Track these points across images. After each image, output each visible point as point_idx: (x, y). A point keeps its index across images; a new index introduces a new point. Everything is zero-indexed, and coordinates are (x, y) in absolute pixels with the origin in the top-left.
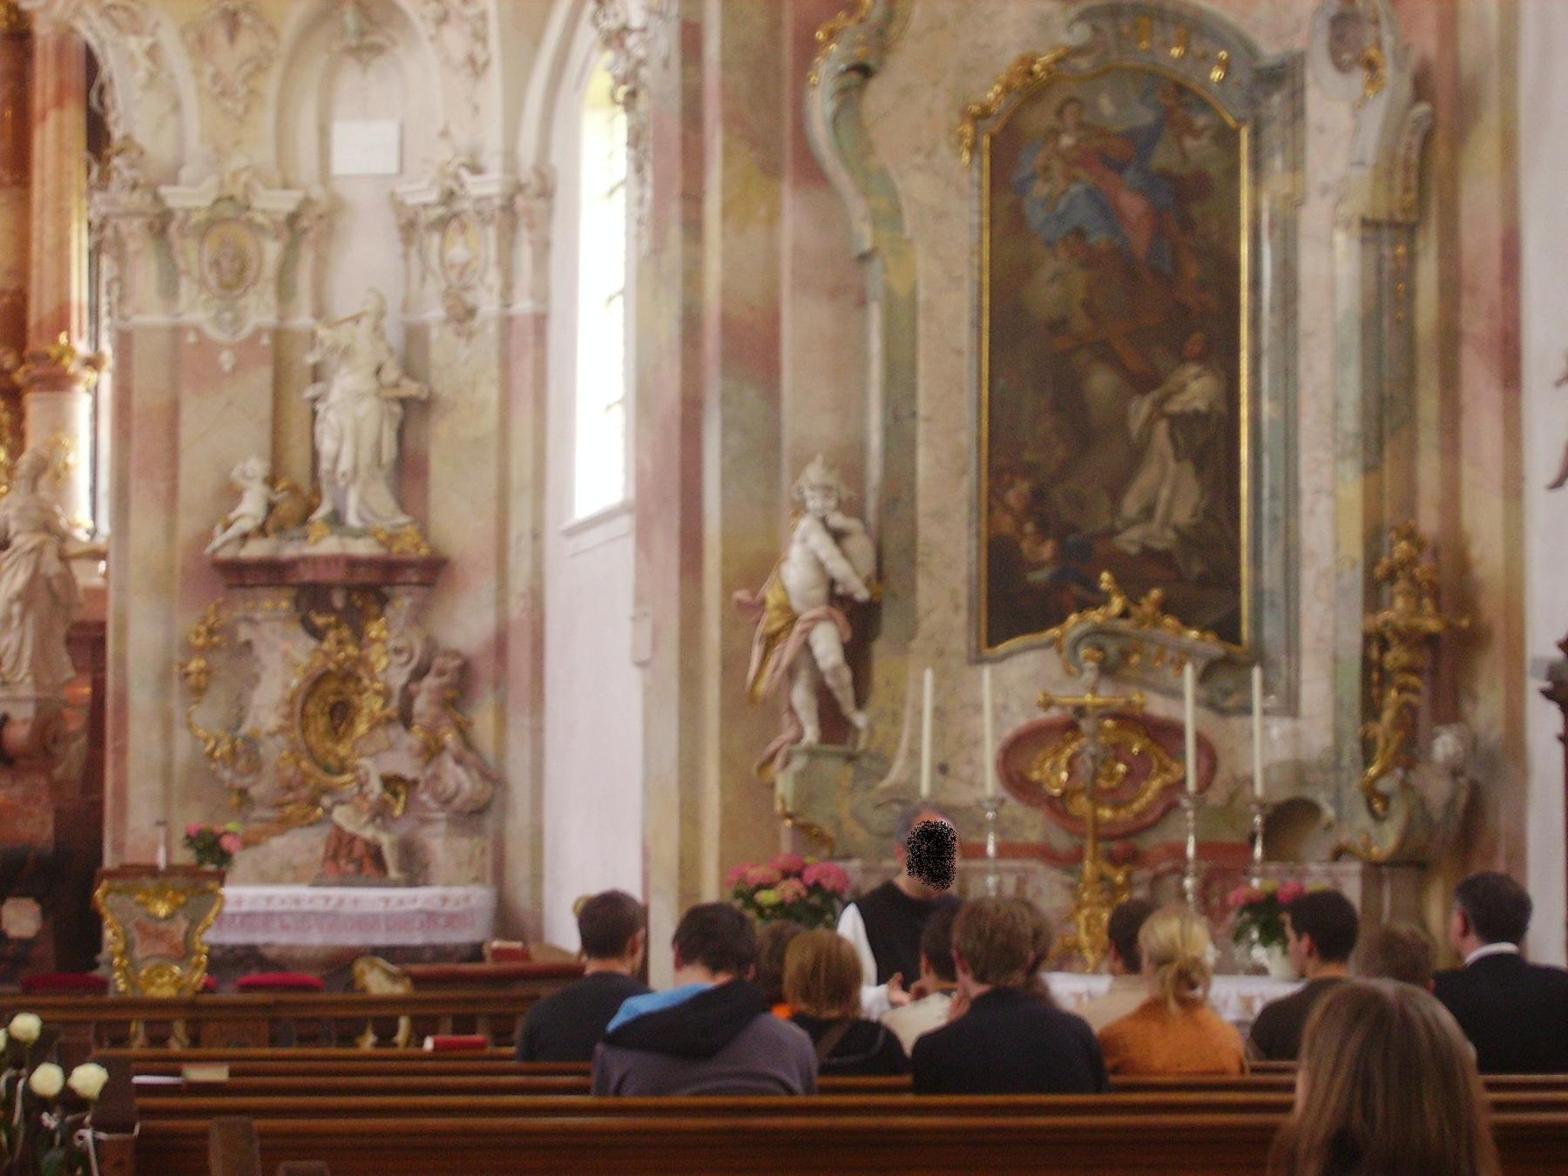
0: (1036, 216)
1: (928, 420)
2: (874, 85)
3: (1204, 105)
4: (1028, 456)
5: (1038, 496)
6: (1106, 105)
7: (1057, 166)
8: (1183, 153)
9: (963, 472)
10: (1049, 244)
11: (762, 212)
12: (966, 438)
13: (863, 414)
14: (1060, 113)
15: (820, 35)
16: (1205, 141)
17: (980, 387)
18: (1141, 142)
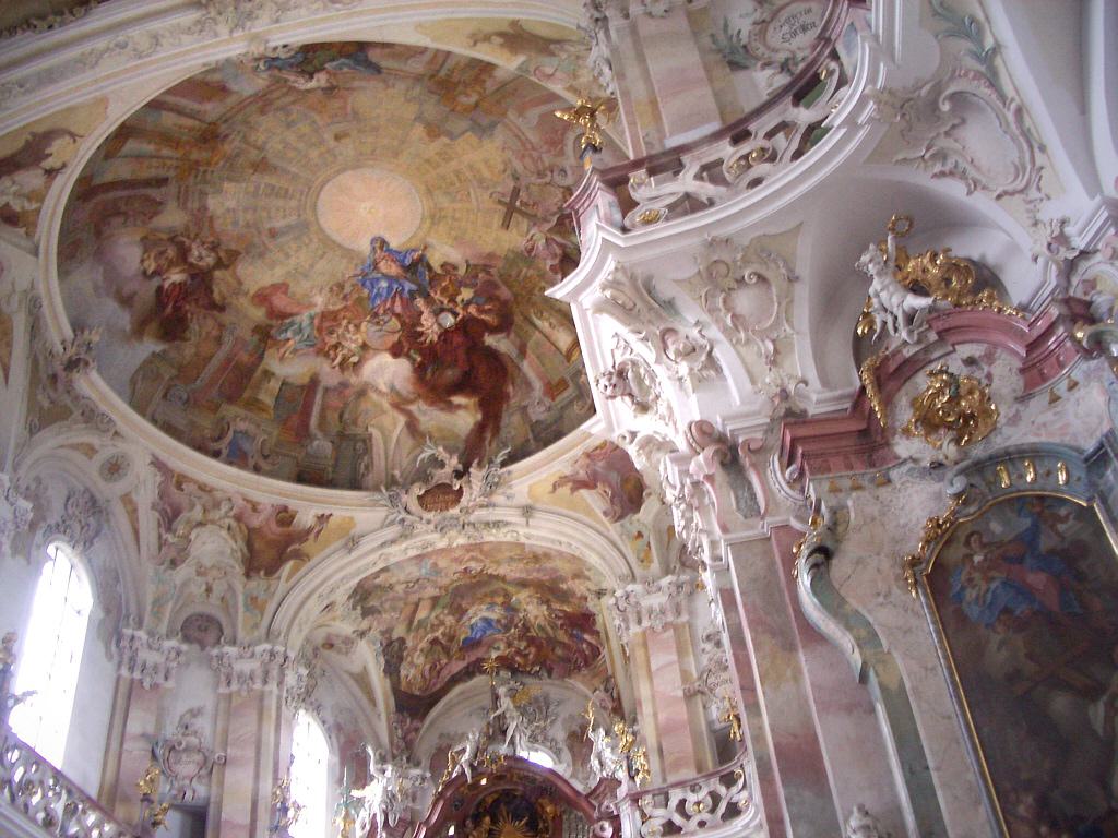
0: (974, 612)
1: (938, 769)
2: (834, 561)
3: (1063, 501)
4: (1024, 776)
5: (1043, 802)
6: (996, 527)
7: (977, 576)
8: (1058, 534)
9: (977, 803)
10: (987, 626)
11: (789, 673)
12: (972, 776)
13: (892, 785)
14: (967, 543)
15: (794, 551)
16: (1071, 522)
17: (971, 737)
18: (1029, 540)
